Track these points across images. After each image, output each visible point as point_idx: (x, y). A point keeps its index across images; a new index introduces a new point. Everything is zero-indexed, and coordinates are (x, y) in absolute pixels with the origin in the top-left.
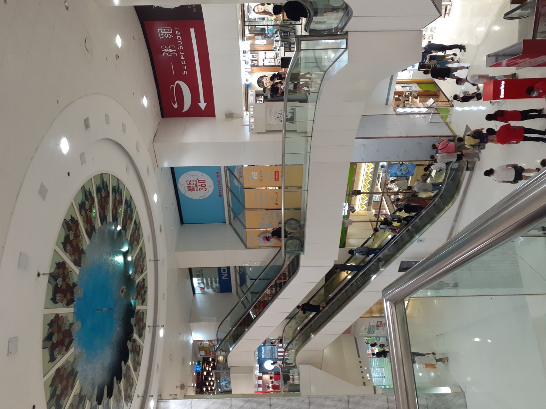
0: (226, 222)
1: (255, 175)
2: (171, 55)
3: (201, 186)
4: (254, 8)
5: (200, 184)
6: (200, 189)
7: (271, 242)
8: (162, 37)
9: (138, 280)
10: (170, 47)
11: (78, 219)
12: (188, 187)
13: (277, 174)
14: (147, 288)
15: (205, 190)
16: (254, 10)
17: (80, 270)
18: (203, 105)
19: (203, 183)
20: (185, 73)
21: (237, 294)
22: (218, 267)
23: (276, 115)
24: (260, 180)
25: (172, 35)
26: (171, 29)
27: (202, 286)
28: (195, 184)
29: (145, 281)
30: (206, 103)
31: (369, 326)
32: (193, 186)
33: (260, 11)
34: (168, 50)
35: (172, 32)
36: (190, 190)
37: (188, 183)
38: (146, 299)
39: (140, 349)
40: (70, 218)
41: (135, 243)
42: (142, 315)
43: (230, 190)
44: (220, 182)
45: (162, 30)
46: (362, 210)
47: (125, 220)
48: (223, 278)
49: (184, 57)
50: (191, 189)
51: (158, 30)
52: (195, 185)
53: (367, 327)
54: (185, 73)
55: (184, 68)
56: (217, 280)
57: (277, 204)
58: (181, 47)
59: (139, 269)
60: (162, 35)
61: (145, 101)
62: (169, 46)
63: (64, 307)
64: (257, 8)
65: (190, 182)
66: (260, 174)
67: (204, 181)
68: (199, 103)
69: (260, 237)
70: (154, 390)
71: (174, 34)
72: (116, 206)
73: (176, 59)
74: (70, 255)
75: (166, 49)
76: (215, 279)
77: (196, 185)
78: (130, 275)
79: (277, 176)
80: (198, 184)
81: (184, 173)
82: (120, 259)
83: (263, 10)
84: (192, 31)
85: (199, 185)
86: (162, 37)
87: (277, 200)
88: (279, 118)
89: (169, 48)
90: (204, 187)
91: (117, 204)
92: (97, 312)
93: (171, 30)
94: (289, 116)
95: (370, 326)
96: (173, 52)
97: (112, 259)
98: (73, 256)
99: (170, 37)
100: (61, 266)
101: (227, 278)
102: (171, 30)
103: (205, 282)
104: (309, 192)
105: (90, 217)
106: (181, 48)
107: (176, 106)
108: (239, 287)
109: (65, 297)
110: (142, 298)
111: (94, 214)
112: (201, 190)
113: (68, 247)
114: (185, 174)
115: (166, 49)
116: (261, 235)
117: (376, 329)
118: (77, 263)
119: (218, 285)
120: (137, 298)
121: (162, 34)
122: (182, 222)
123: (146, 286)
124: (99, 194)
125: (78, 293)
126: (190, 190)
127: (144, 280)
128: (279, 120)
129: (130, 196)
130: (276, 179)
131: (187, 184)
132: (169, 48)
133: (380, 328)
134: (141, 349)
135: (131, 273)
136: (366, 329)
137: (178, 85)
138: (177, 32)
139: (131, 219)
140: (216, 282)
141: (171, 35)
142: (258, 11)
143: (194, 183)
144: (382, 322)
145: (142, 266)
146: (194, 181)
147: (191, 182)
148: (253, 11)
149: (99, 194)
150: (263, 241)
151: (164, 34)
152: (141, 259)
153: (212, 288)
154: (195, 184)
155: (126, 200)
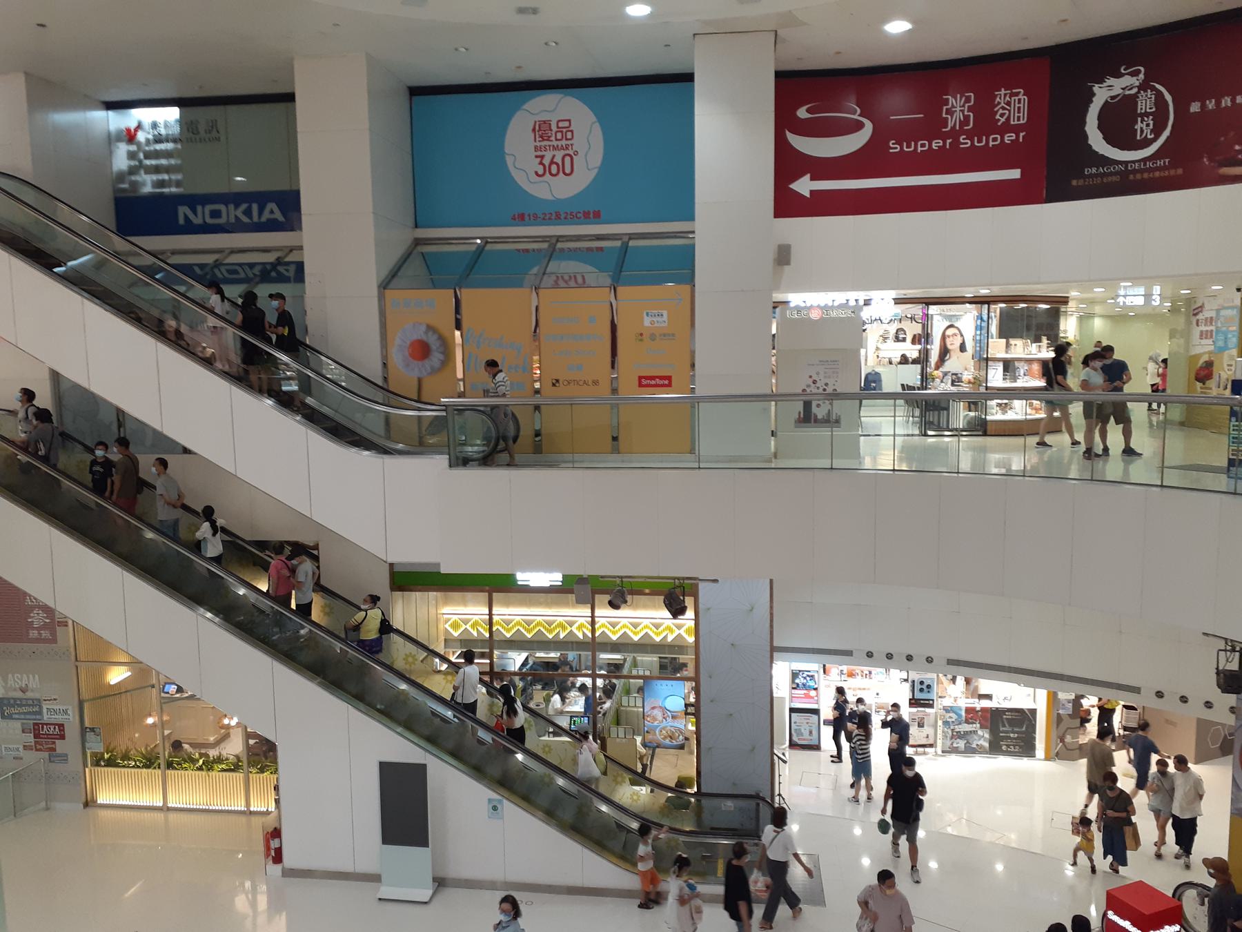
0: (418, 230)
1: (659, 319)
2: (944, 116)
3: (552, 162)
4: (957, 328)
5: (558, 159)
6: (542, 157)
7: (407, 365)
8: (1000, 98)
10: (969, 115)
12: (546, 123)
13: (661, 382)
15: (537, 173)
16: (951, 326)
18: (804, 186)
19: (561, 169)
20: (894, 147)
22: (297, 193)
23: (821, 376)
24: (641, 335)
25: (1003, 123)
26: (1022, 122)
27: (141, 136)
28: (559, 143)
30: (808, 196)
31: (39, 700)
32: (553, 138)
33: (948, 342)
34: (960, 110)
35: (1012, 123)
36: (537, 128)
37: (561, 124)
43: (553, 248)
44: (565, 218)
45: (1019, 100)
46: (447, 626)
49: (937, 148)
50: (542, 130)
51: (1022, 91)
52: (555, 143)
53: (29, 695)
54: (894, 147)
55: (908, 146)
56: (174, 190)
57: (554, 385)
58: (896, 148)
60: (1004, 98)
61: (897, 27)
62: (971, 114)
64: (955, 335)
65: (564, 130)
66: (660, 335)
67: (568, 170)
68: (808, 176)
69: (426, 333)
71: (1007, 128)
73: (933, 126)
75: (963, 106)
76: (178, 184)
77: (555, 148)
79: (653, 382)
80: (558, 156)
81: (597, 118)
83: (949, 347)
84: (1015, 174)
85: (554, 156)
86: (1000, 98)
87: (569, 383)
88: (813, 385)
89: (966, 113)
90: (547, 170)
93: (1019, 120)
94: (819, 412)
95: (37, 703)
96: (953, 122)
99: (998, 117)
102: (1019, 120)
103: (159, 147)
104: (697, 471)
106: (965, 143)
107: (802, 113)
112: (539, 159)
114: (594, 119)
115: (963, 106)
116: (435, 337)
117: (23, 724)
119: (148, 189)
121: (1008, 98)
126: (537, 128)
128: (808, 386)
130: (643, 380)
131: (559, 121)
132: (966, 113)
133: (30, 738)
136: (23, 691)
137: (859, 126)
138: (1012, 136)
140: (161, 184)
141: (1003, 120)
142: (949, 337)
143: (564, 143)
144: (62, 737)
146: (569, 142)
147: (566, 130)
148: (948, 323)
150: (408, 343)
151: (1008, 104)
153: (132, 171)
154: (559, 143)
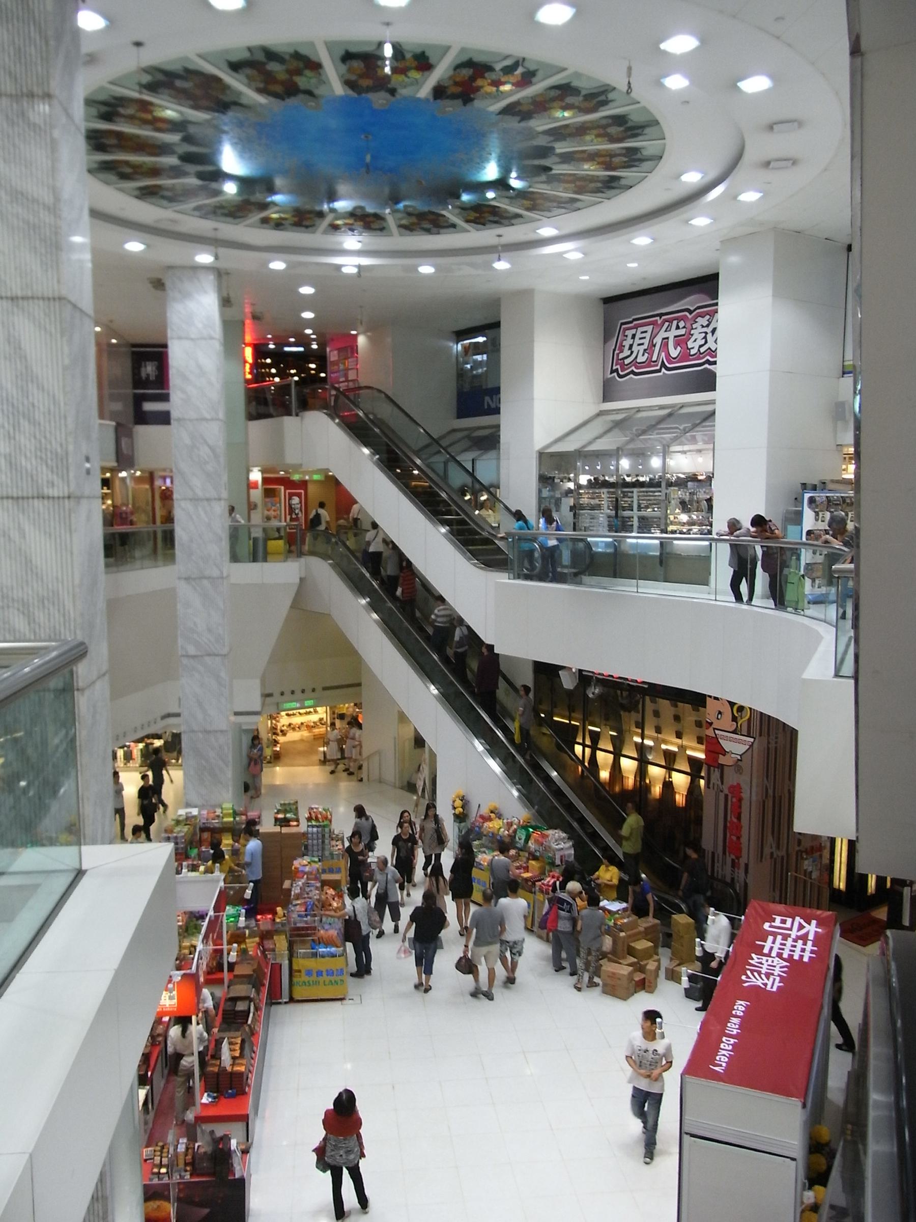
9: (449, 213)
11: (535, 84)
14: (438, 233)
17: (427, 100)
21: (454, 431)
29: (452, 229)
38: (415, 233)
39: (307, 227)
40: (532, 67)
41: (527, 203)
42: (377, 227)
47: (570, 178)
48: (487, 399)
59: (473, 215)
63: (341, 77)
70: (235, 260)
72: (596, 159)
74: (450, 78)
78: (458, 197)
82: (491, 171)
91: (601, 159)
92: (363, 137)
97: (494, 155)
98: (451, 82)
100: (423, 62)
101: (486, 407)
105: (551, 108)
108: (465, 433)
109: (361, 76)
110: (413, 224)
111: (559, 114)
113: (467, 72)
118: (439, 92)
120: (409, 214)
122: (608, 301)
123: (442, 231)
124: (610, 121)
125: (379, 99)
127: (454, 226)
129: (631, 185)
134: (310, 229)
135: (465, 197)
139: (580, 191)
145: (482, 220)
149: (610, 121)
152: (496, 219)
155: (618, 178)
